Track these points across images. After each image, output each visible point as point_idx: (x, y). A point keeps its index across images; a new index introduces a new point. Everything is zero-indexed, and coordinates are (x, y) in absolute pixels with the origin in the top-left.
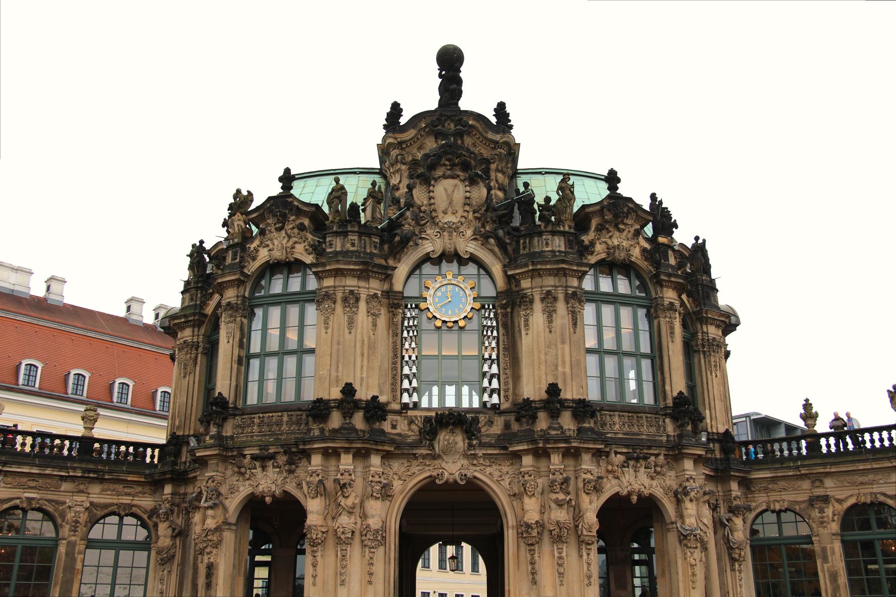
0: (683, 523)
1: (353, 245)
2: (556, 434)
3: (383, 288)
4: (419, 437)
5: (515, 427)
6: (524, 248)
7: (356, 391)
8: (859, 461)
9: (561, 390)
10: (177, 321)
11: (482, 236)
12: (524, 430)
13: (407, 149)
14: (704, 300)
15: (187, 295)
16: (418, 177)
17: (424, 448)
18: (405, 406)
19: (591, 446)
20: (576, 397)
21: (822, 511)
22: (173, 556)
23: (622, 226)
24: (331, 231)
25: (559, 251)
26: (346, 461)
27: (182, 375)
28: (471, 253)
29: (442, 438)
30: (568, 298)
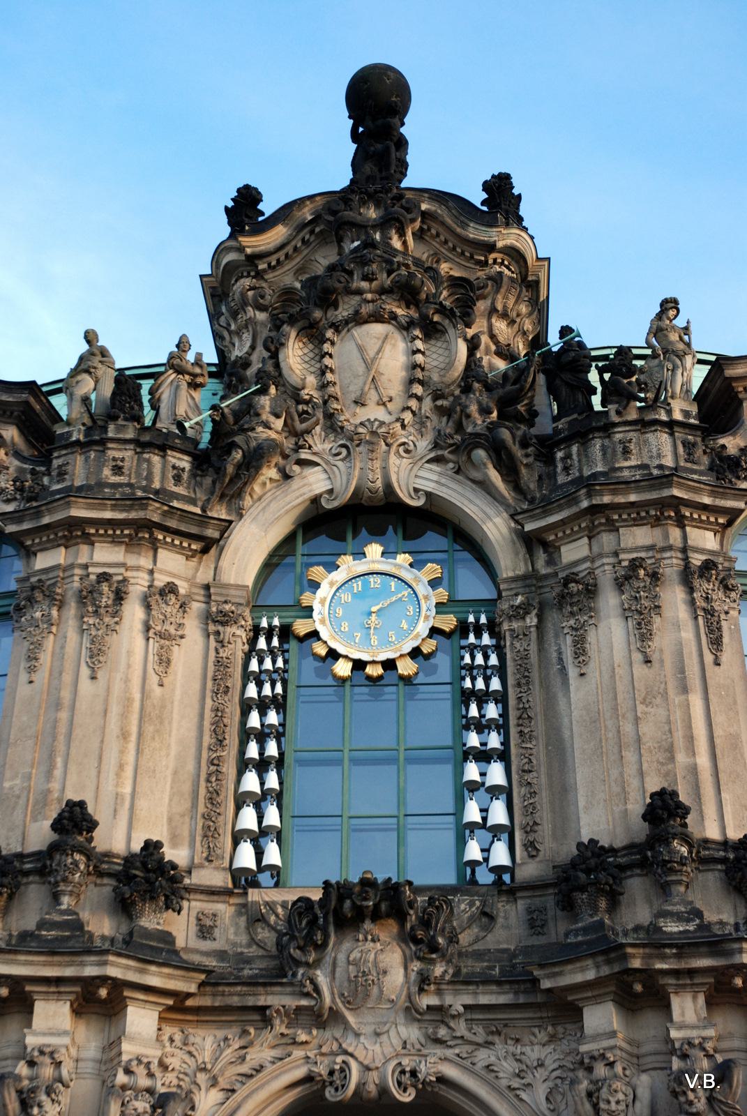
1: (118, 470)
2: (680, 932)
3: (194, 577)
4: (273, 963)
5: (559, 929)
6: (566, 469)
7: (92, 825)
9: (687, 811)
11: (456, 449)
12: (585, 930)
13: (269, 276)
16: (292, 321)
17: (289, 989)
24: (64, 443)
28: (429, 495)
29: (341, 957)
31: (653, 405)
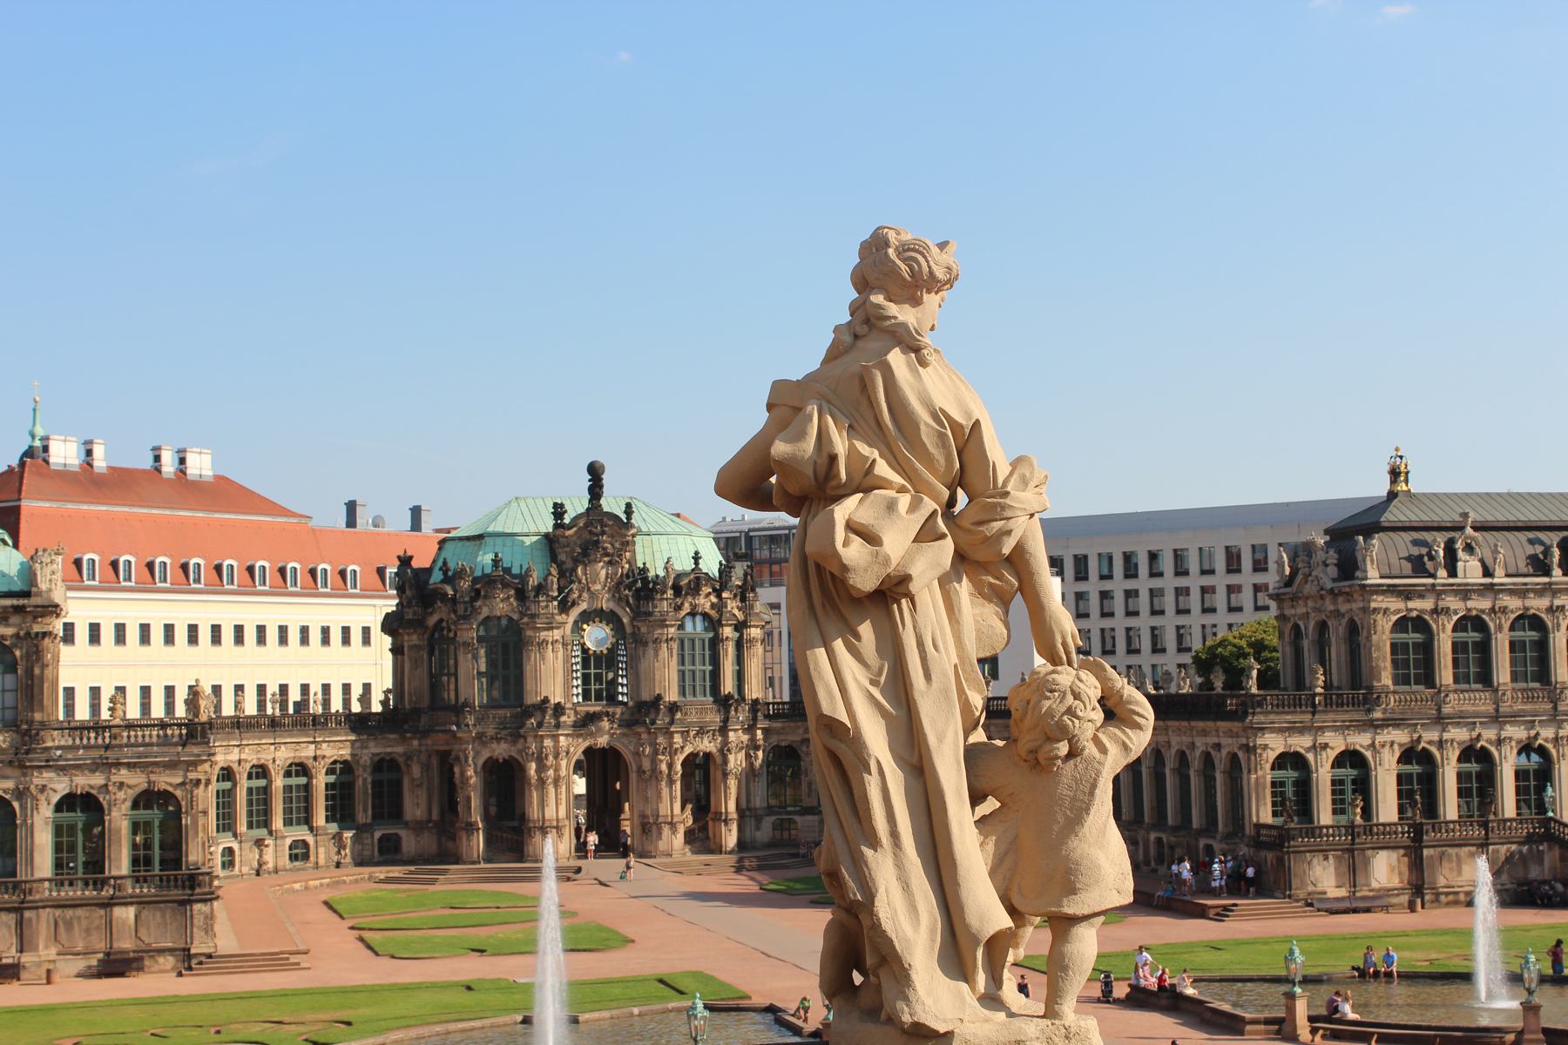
15: (411, 611)
18: (574, 704)
22: (422, 784)
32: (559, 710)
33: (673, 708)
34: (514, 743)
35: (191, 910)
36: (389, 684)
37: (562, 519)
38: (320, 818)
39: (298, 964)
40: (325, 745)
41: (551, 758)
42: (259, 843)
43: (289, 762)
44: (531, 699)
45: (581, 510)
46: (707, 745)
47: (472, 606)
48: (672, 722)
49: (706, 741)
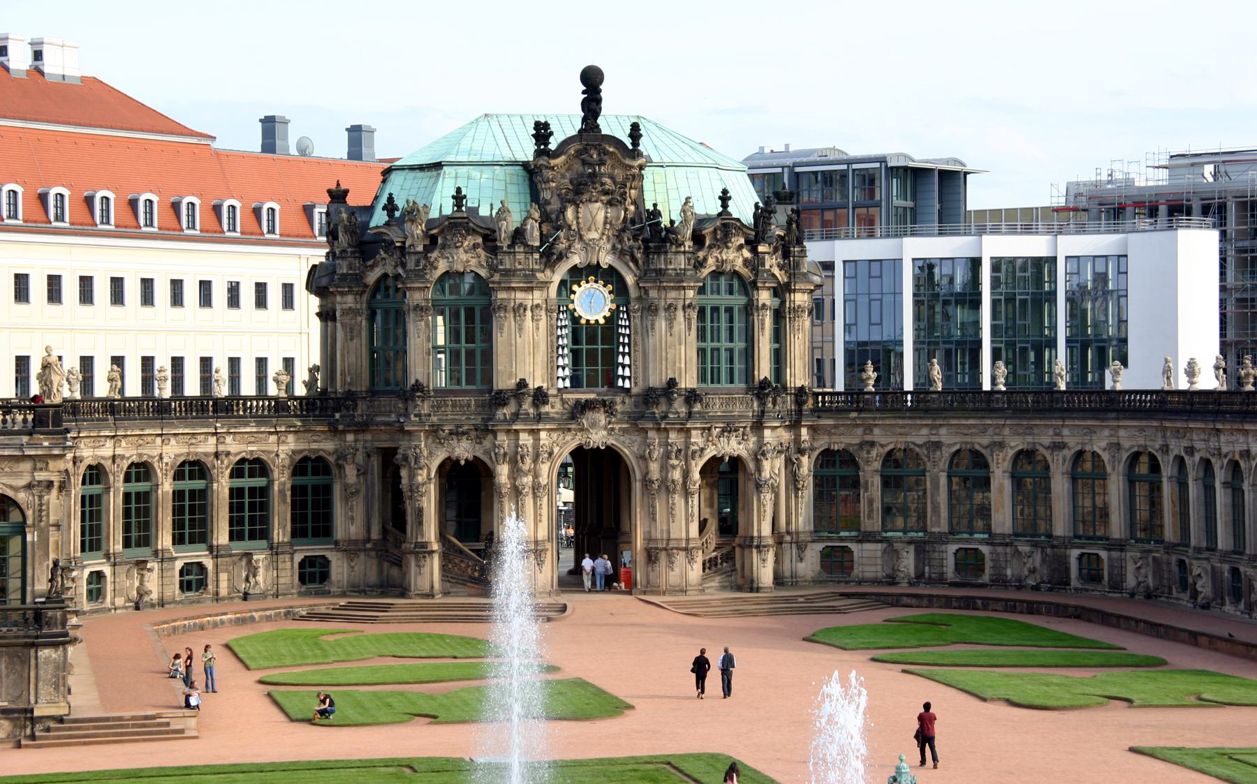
0: (760, 475)
1: (520, 263)
8: (899, 418)
10: (339, 289)
14: (794, 270)
18: (559, 390)
19: (698, 426)
20: (688, 386)
21: (868, 452)
22: (359, 491)
23: (730, 245)
25: (680, 269)
26: (525, 439)
27: (349, 338)
29: (590, 418)
30: (684, 308)
31: (680, 245)
32: (540, 397)
33: (692, 397)
34: (479, 440)
35: (36, 658)
36: (316, 360)
37: (547, 144)
38: (221, 536)
39: (182, 731)
40: (229, 439)
41: (528, 460)
42: (141, 564)
43: (182, 459)
44: (504, 382)
45: (574, 132)
46: (733, 446)
47: (426, 258)
48: (690, 415)
49: (733, 441)
